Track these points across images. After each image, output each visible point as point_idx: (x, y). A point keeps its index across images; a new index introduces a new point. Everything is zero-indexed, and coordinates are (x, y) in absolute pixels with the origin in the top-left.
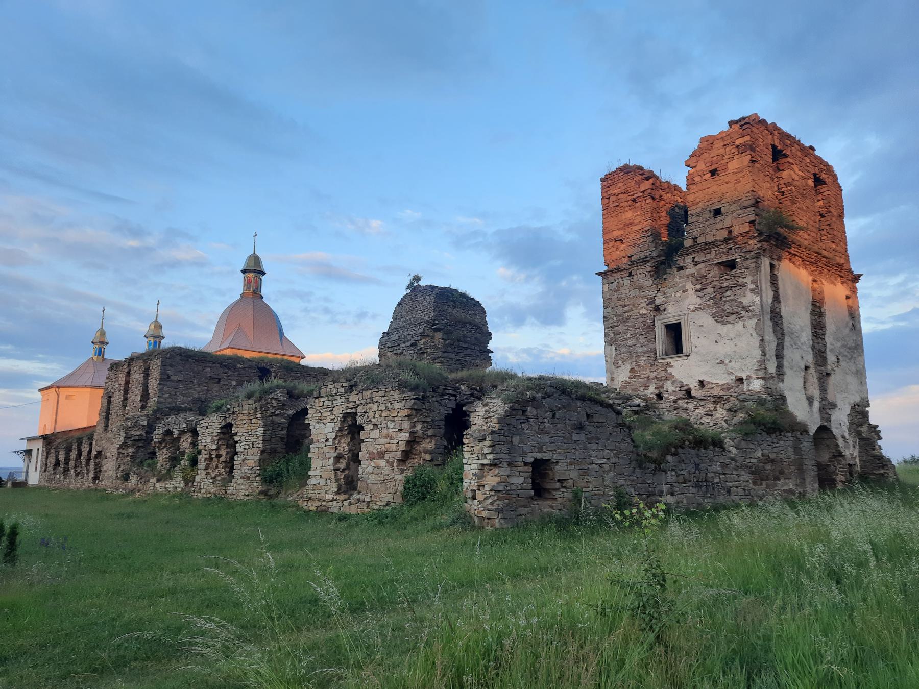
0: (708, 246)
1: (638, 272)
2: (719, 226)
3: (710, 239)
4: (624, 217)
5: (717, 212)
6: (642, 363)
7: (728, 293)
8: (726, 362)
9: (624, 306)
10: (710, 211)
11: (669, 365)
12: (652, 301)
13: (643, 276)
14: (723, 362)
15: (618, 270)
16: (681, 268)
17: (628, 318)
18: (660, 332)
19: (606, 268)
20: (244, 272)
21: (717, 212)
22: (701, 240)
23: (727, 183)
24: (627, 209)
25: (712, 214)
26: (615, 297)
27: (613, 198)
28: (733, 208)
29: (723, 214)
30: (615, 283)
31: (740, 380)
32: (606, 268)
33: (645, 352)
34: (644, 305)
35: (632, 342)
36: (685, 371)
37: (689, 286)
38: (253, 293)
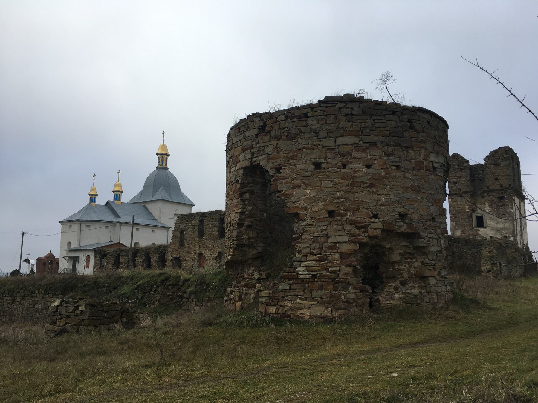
0: (494, 190)
3: (494, 187)
6: (466, 229)
11: (478, 230)
13: (467, 197)
16: (483, 197)
17: (461, 212)
18: (474, 219)
20: (158, 154)
22: (490, 188)
26: (454, 204)
28: (503, 178)
31: (506, 237)
35: (462, 221)
36: (485, 232)
37: (487, 204)
38: (162, 166)
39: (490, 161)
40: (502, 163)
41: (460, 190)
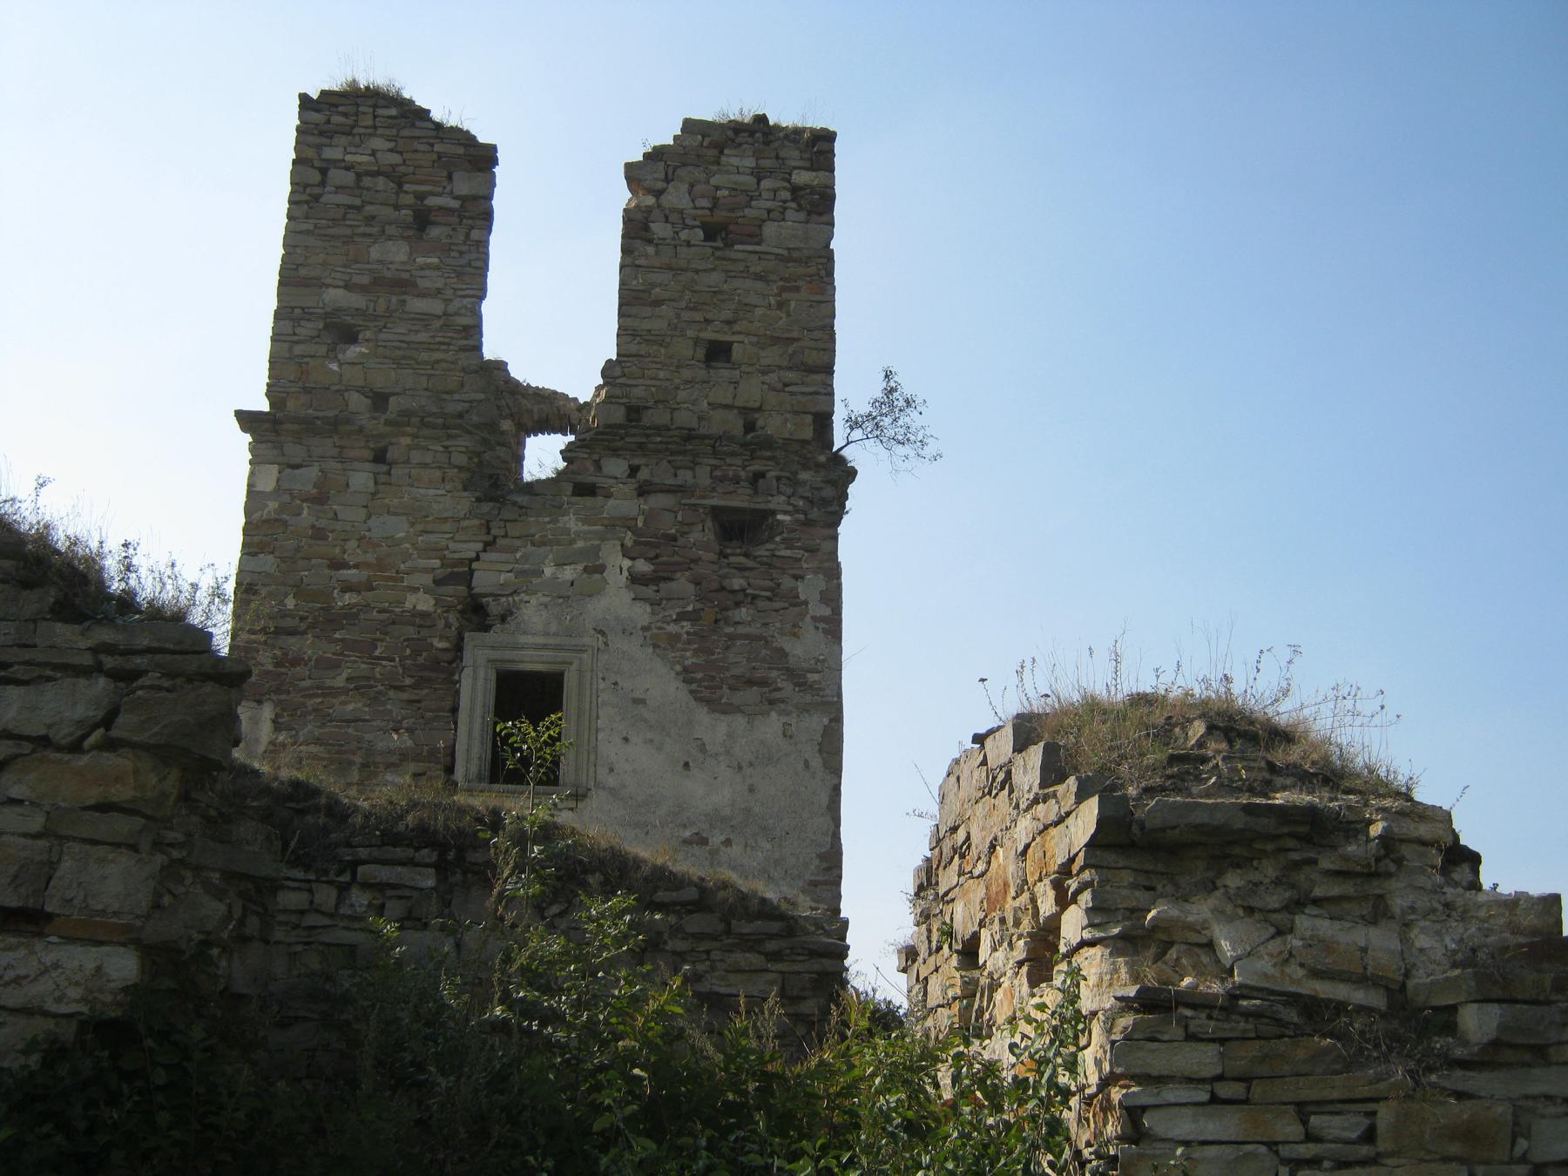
1: (416, 457)
2: (722, 395)
4: (375, 252)
5: (717, 353)
7: (743, 613)
8: (717, 839)
9: (337, 565)
10: (697, 341)
12: (461, 574)
14: (702, 841)
15: (334, 426)
17: (350, 616)
18: (475, 689)
19: (264, 406)
21: (717, 353)
23: (758, 277)
24: (391, 230)
25: (701, 353)
27: (337, 176)
28: (770, 356)
29: (735, 366)
30: (312, 473)
32: (264, 406)
33: (404, 756)
34: (427, 579)
39: (677, 197)
40: (770, 230)
41: (379, 400)
